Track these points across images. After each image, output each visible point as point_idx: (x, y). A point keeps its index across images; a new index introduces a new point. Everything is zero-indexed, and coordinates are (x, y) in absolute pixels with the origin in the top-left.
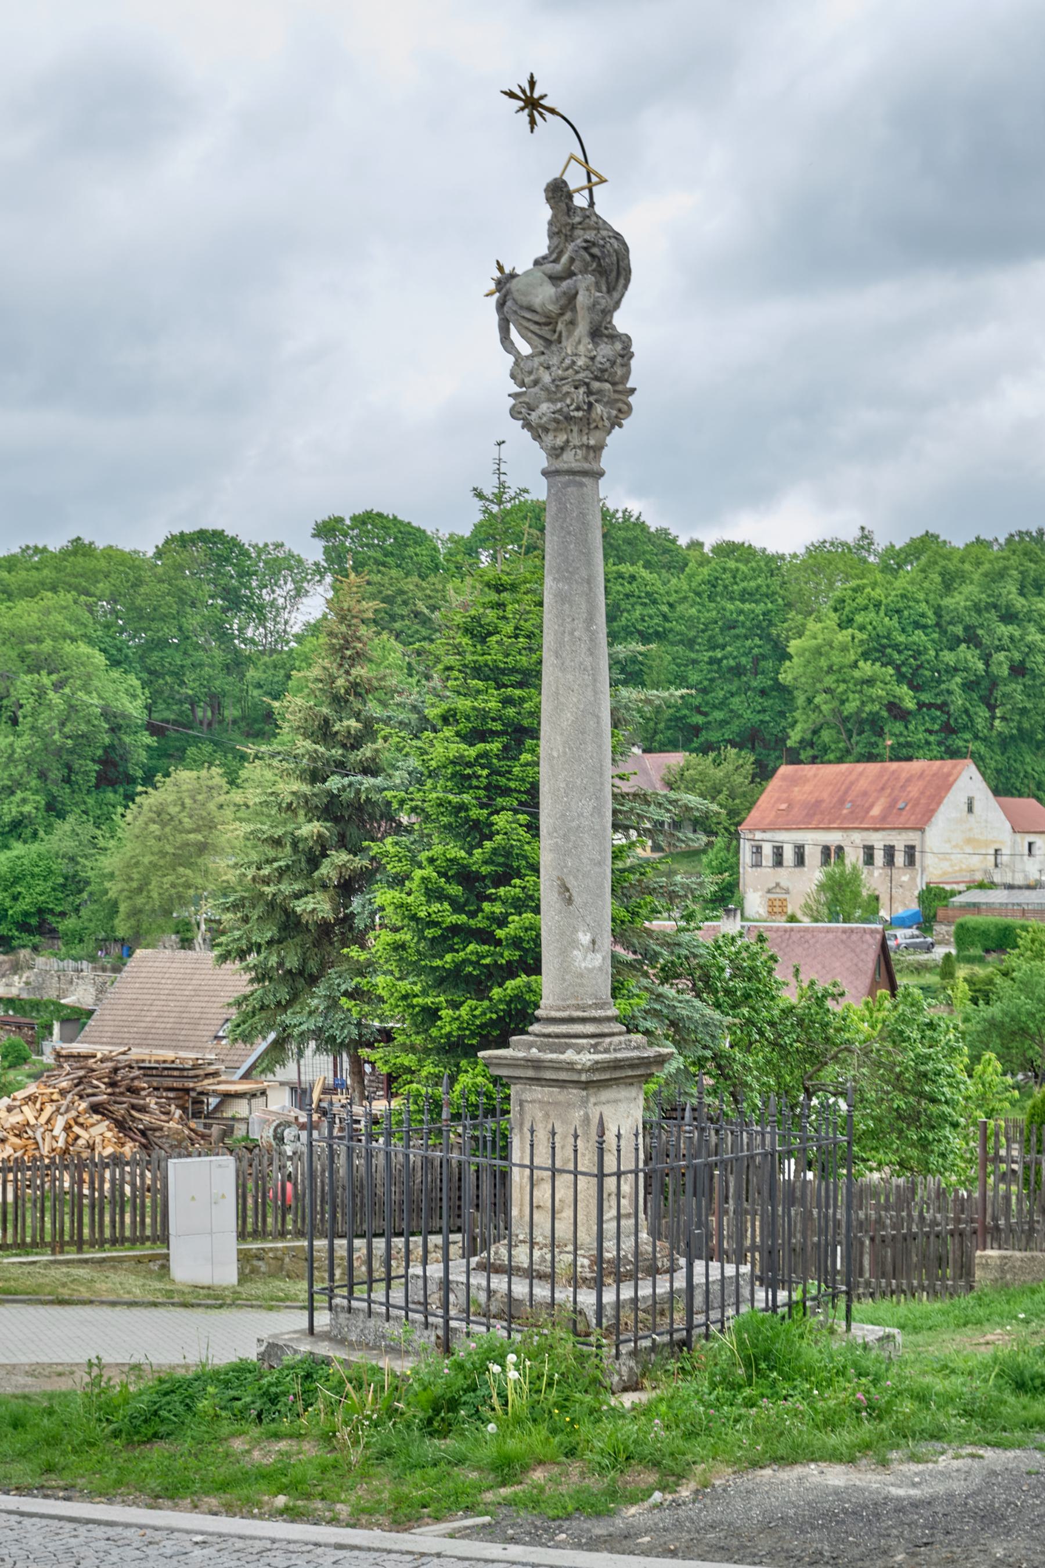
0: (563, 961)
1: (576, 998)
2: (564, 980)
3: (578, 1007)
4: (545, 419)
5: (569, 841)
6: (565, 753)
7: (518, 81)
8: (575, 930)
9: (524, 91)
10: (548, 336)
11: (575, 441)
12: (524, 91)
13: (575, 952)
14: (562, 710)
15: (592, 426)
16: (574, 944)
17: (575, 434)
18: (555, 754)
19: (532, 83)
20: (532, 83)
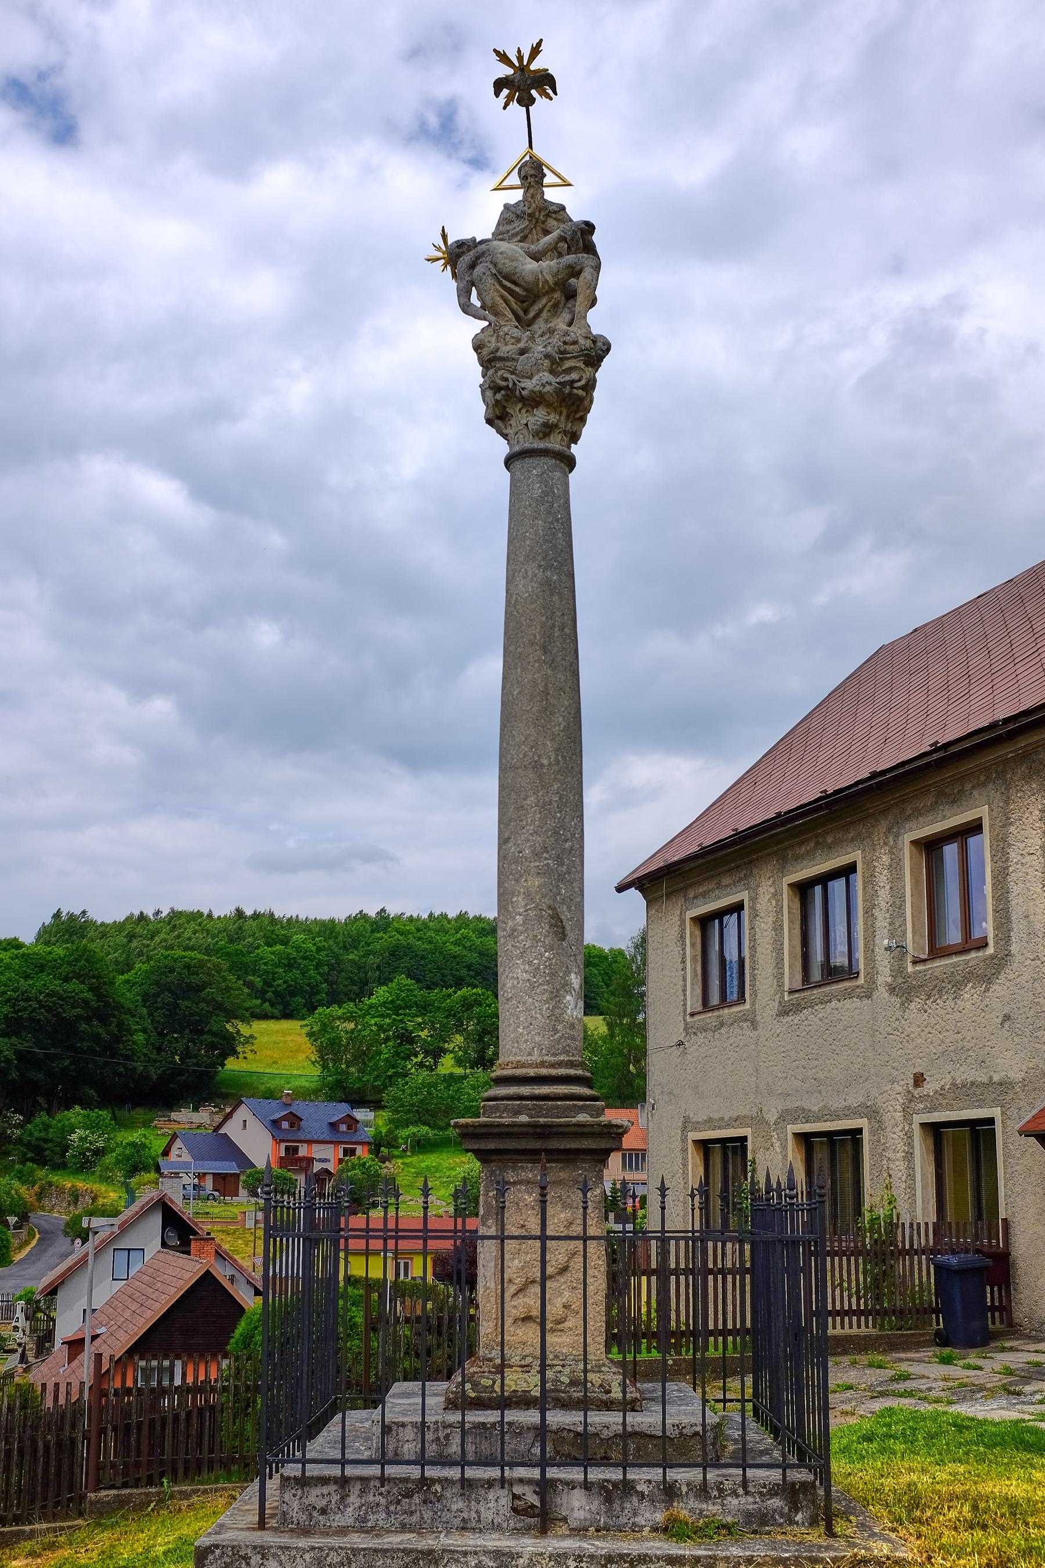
0: (554, 1008)
1: (567, 1053)
2: (556, 1031)
3: (571, 1064)
4: (548, 388)
5: (562, 865)
6: (558, 762)
7: (516, 44)
8: (568, 972)
9: (520, 58)
10: (521, 313)
11: (562, 425)
12: (520, 58)
13: (568, 998)
14: (552, 713)
15: (578, 415)
16: (566, 985)
17: (563, 418)
18: (545, 762)
19: (536, 51)
20: (536, 51)
